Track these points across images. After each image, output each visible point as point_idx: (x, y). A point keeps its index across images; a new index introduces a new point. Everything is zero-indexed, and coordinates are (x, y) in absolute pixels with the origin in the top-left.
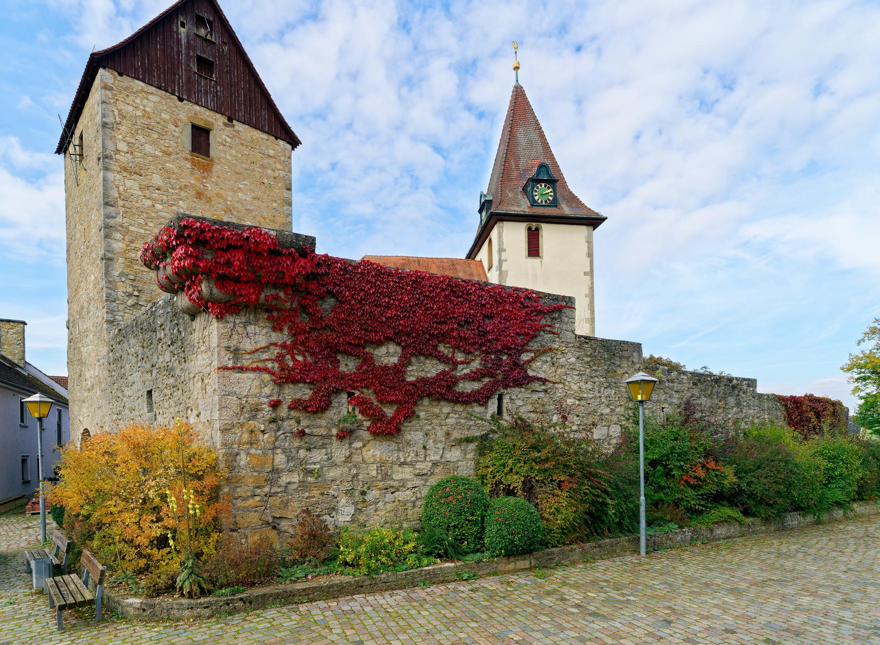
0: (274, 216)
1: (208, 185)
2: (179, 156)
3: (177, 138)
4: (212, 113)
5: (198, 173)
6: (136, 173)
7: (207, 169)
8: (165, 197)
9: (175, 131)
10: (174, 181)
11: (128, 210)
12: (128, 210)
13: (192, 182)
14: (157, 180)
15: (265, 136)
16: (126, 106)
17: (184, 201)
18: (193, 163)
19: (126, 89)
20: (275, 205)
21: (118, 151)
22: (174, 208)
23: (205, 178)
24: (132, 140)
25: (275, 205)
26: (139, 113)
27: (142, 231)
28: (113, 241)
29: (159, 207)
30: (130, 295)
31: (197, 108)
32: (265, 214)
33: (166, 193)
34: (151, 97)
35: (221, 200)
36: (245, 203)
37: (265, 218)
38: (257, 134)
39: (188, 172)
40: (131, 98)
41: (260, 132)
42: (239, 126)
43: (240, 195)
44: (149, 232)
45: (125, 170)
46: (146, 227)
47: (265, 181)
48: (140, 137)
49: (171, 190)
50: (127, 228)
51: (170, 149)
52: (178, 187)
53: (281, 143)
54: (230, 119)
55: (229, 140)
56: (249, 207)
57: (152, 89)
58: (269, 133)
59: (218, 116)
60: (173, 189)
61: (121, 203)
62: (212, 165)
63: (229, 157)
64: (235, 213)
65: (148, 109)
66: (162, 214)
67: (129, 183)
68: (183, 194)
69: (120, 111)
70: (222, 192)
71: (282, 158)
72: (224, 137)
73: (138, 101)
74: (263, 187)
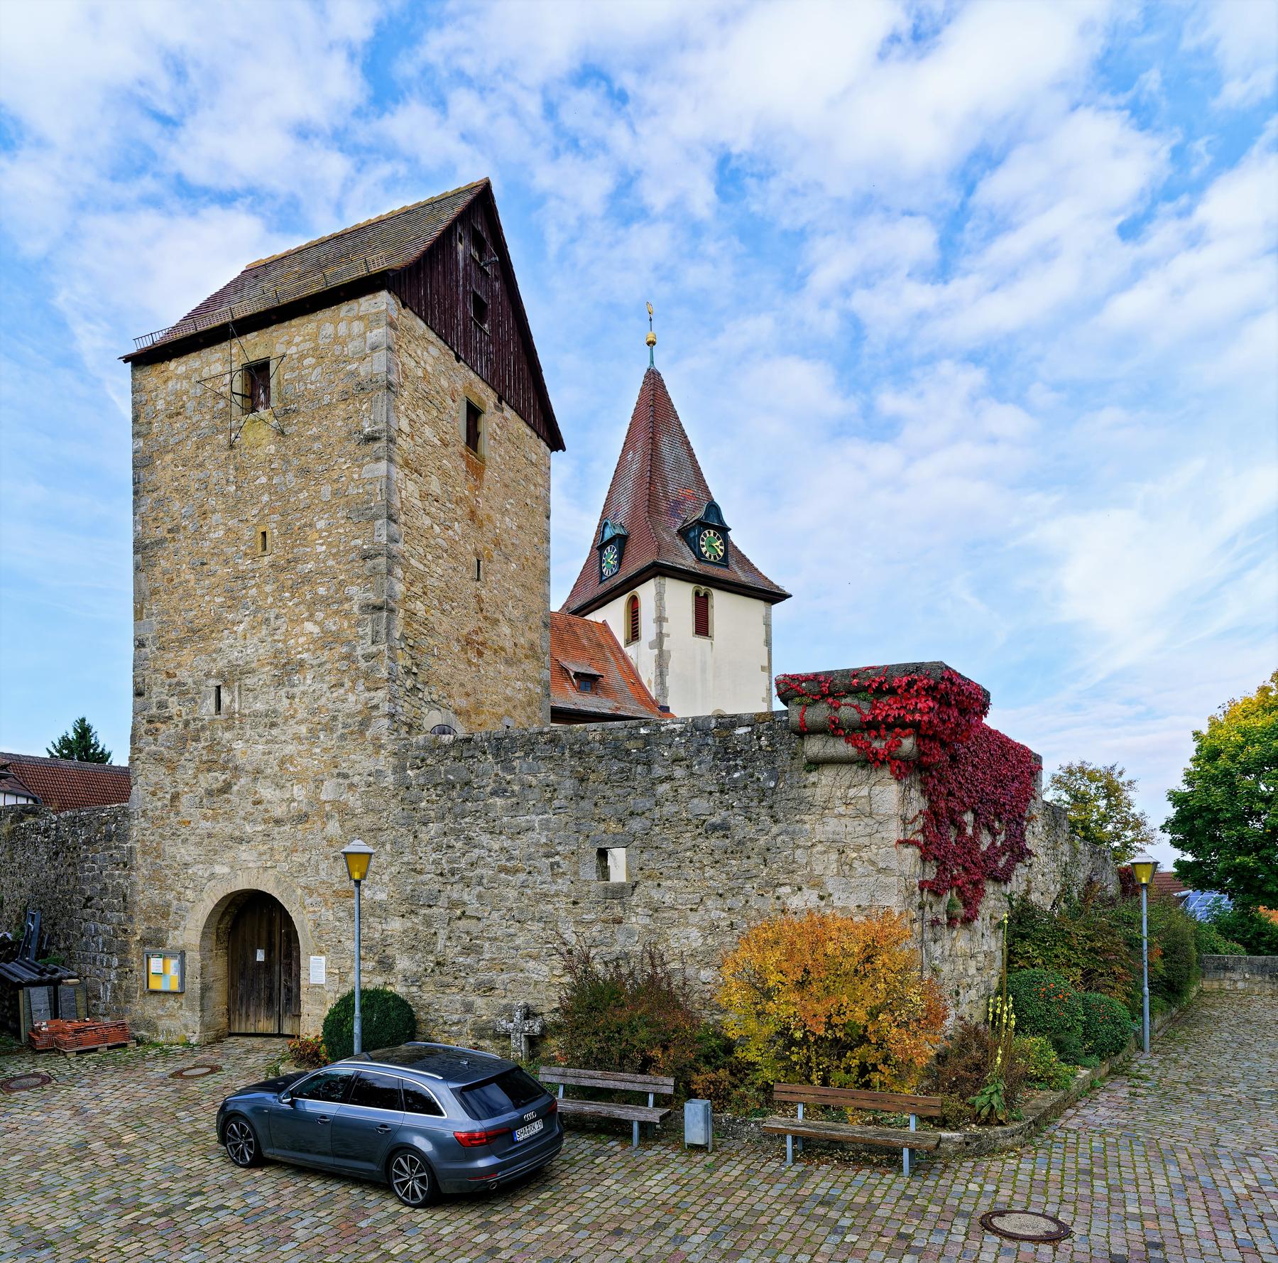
10: (450, 489)
11: (409, 531)
12: (409, 531)
13: (466, 492)
14: (435, 487)
17: (459, 522)
22: (450, 532)
27: (421, 567)
28: (394, 580)
30: (408, 672)
33: (443, 508)
44: (427, 570)
46: (426, 562)
49: (448, 504)
50: (408, 560)
52: (454, 499)
66: (439, 540)
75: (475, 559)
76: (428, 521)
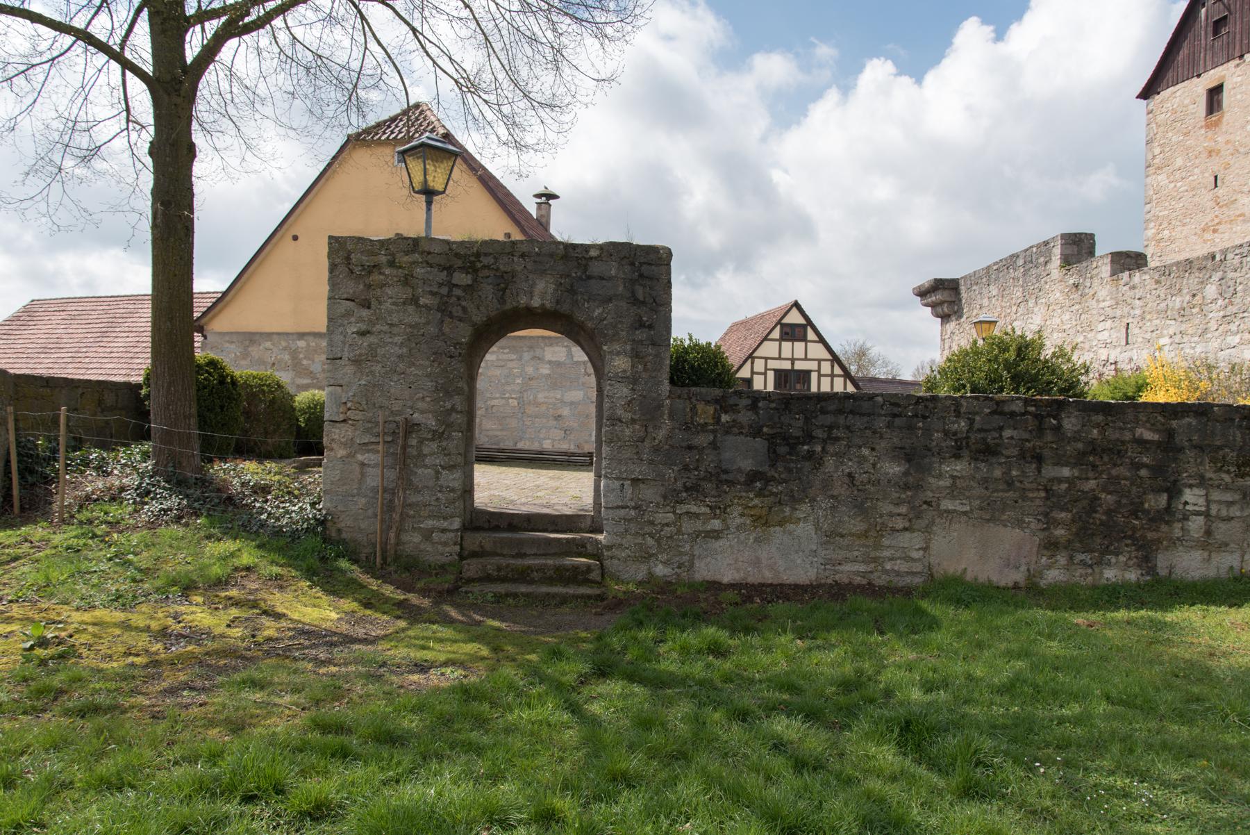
7: (1217, 124)
8: (1184, 174)
14: (1179, 162)
18: (1207, 126)
27: (1167, 212)
29: (1179, 184)
34: (1178, 94)
35: (1229, 146)
39: (1202, 139)
45: (1159, 168)
55: (1239, 79)
57: (1178, 87)
61: (1154, 197)
62: (1222, 117)
67: (1160, 178)
68: (1197, 161)
70: (1231, 137)
75: (1212, 179)
76: (1172, 185)
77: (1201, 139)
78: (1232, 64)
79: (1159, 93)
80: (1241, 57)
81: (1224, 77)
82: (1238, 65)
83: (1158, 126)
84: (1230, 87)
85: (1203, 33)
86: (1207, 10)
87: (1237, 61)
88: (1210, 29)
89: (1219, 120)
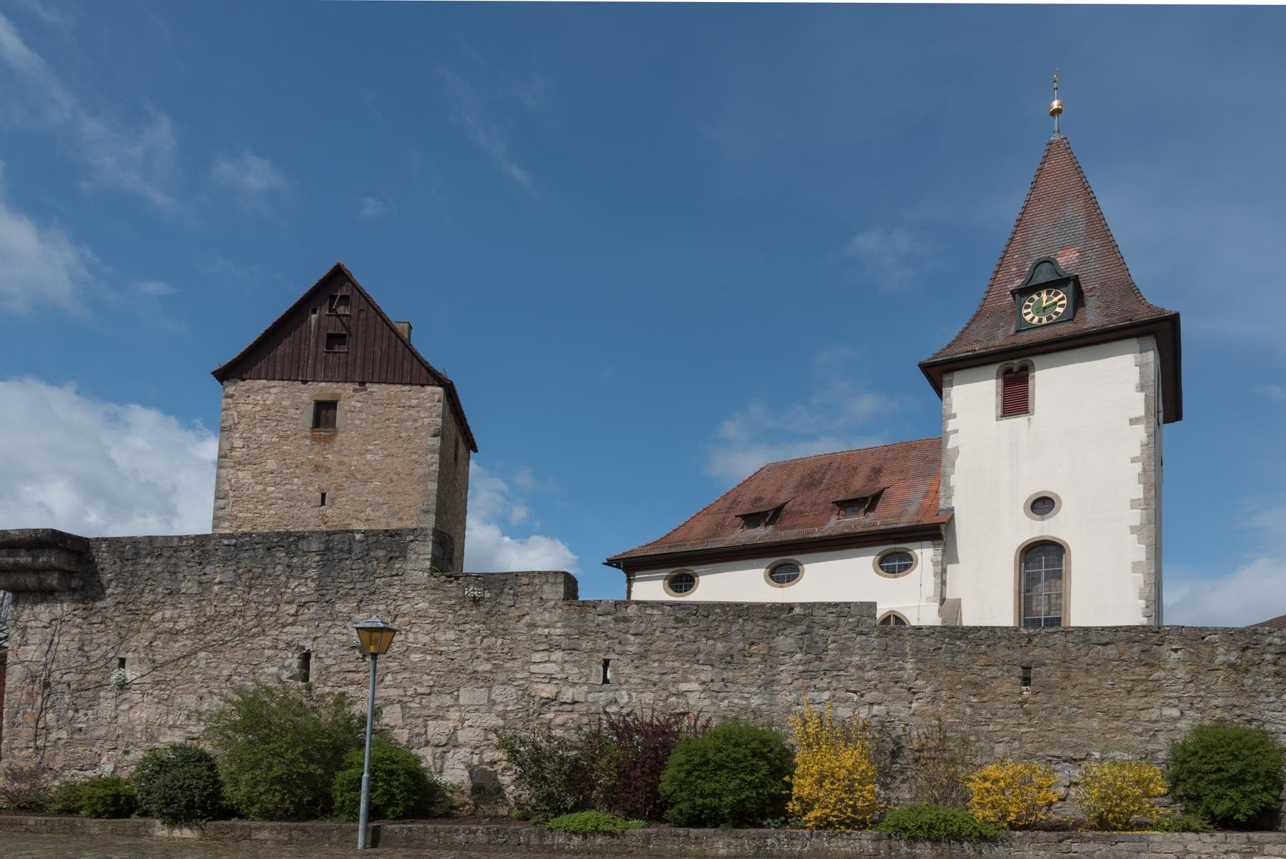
0: (412, 469)
1: (330, 456)
2: (297, 436)
3: (298, 419)
4: (340, 384)
5: (317, 447)
6: (250, 464)
7: (328, 440)
9: (296, 414)
13: (310, 457)
14: (271, 464)
15: (407, 388)
16: (246, 406)
18: (314, 439)
19: (248, 390)
20: (414, 457)
21: (233, 449)
23: (325, 450)
24: (248, 435)
25: (414, 457)
26: (258, 408)
31: (323, 384)
32: (400, 469)
34: (273, 390)
35: (343, 468)
36: (374, 464)
37: (399, 474)
38: (395, 389)
39: (306, 449)
40: (252, 397)
41: (399, 386)
42: (372, 388)
43: (369, 456)
47: (404, 435)
48: (259, 431)
49: (285, 471)
51: (289, 432)
52: (294, 466)
53: (429, 389)
54: (362, 383)
55: (359, 405)
56: (379, 467)
58: (411, 384)
59: (347, 385)
60: (288, 469)
63: (357, 422)
64: (359, 476)
65: (268, 402)
68: (298, 471)
69: (239, 412)
70: (346, 459)
71: (429, 404)
72: (353, 403)
73: (259, 398)
74: (400, 441)
77: (304, 448)
78: (350, 387)
79: (244, 380)
80: (362, 383)
81: (340, 395)
82: (355, 390)
83: (241, 416)
84: (347, 408)
85: (312, 340)
86: (319, 319)
87: (357, 386)
88: (323, 340)
89: (330, 436)
